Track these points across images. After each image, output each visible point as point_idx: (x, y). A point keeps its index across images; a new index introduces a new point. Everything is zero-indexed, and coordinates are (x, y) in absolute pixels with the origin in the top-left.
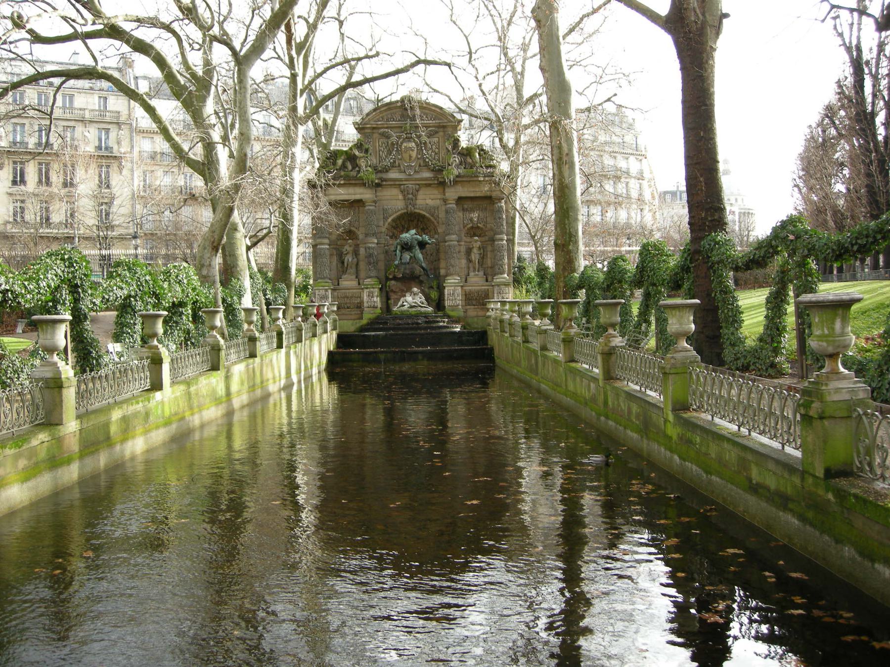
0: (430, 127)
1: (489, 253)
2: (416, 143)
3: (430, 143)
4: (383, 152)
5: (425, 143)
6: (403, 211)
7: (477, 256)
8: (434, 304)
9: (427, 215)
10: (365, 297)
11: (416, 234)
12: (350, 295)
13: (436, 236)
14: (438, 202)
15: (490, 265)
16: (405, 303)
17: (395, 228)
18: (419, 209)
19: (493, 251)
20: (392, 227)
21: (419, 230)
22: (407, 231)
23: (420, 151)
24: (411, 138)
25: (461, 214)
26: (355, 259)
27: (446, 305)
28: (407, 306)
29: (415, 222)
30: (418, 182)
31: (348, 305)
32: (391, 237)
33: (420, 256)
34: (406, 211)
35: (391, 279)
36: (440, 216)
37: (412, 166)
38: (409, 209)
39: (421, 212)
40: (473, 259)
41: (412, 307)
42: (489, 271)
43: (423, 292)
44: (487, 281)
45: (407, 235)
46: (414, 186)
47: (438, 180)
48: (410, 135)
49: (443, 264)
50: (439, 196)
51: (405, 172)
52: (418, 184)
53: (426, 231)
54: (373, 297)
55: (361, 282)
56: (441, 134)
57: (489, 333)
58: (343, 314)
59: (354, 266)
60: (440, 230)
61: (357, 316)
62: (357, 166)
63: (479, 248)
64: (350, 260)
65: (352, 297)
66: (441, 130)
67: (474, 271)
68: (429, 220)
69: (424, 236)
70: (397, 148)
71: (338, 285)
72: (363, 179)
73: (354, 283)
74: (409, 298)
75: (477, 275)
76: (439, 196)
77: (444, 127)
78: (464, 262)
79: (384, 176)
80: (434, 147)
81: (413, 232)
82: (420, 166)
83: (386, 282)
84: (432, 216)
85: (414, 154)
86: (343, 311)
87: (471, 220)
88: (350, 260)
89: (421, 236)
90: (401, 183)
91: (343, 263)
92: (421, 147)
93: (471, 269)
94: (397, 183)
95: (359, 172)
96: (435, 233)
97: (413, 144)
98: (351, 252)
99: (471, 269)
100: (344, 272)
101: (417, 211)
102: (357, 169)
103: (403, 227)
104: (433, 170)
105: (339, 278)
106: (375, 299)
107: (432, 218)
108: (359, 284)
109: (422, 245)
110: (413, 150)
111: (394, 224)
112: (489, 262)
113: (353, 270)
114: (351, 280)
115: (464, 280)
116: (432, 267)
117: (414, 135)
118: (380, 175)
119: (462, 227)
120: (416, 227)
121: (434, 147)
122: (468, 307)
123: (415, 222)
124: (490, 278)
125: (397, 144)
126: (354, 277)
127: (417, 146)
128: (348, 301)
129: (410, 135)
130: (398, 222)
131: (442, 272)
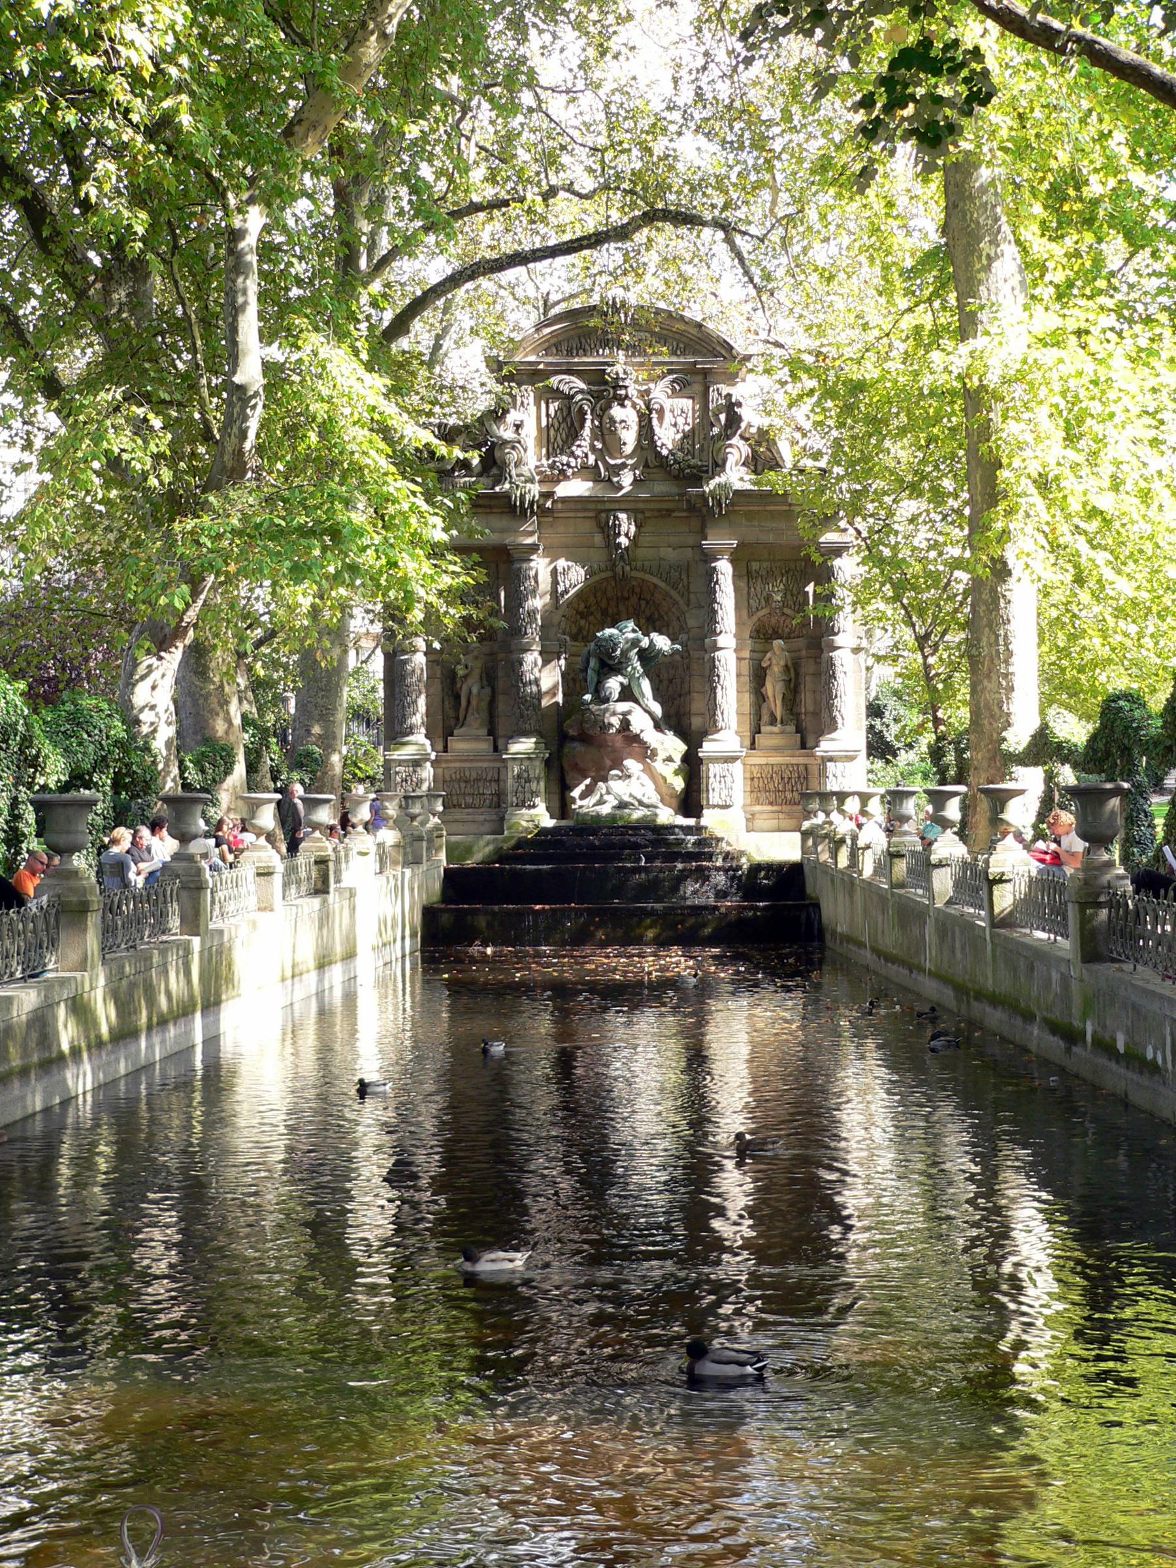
1: (808, 678)
3: (672, 411)
4: (557, 431)
5: (661, 412)
6: (603, 575)
7: (780, 687)
8: (675, 802)
9: (663, 585)
10: (510, 781)
12: (474, 775)
13: (683, 637)
14: (689, 553)
15: (810, 708)
17: (582, 615)
18: (643, 570)
19: (817, 674)
20: (578, 612)
21: (643, 621)
23: (646, 431)
24: (627, 396)
25: (743, 584)
26: (488, 690)
27: (704, 803)
28: (612, 802)
29: (634, 600)
30: (641, 506)
31: (469, 800)
32: (574, 638)
33: (646, 685)
34: (609, 574)
35: (573, 739)
36: (692, 588)
38: (619, 569)
39: (647, 577)
40: (770, 694)
41: (622, 805)
42: (808, 722)
43: (649, 771)
44: (803, 746)
47: (689, 502)
48: (623, 392)
49: (697, 704)
50: (691, 540)
51: (610, 480)
52: (642, 512)
53: (658, 624)
54: (528, 780)
55: (501, 742)
56: (698, 388)
57: (806, 870)
58: (457, 821)
59: (484, 705)
60: (692, 623)
61: (487, 827)
62: (495, 462)
64: (475, 690)
65: (477, 780)
66: (700, 378)
67: (773, 721)
68: (667, 595)
69: (653, 635)
71: (445, 750)
72: (510, 498)
73: (485, 746)
74: (618, 786)
76: (691, 540)
77: (705, 373)
78: (747, 698)
80: (681, 421)
81: (631, 625)
82: (646, 466)
83: (561, 746)
84: (675, 587)
86: (458, 814)
87: (768, 599)
88: (475, 690)
90: (600, 507)
91: (457, 697)
92: (650, 419)
93: (765, 718)
94: (591, 506)
95: (499, 480)
96: (682, 629)
98: (476, 674)
99: (765, 718)
100: (460, 721)
101: (634, 574)
102: (494, 471)
103: (605, 613)
104: (676, 478)
105: (448, 733)
106: (534, 786)
107: (673, 593)
108: (496, 749)
109: (647, 656)
111: (582, 606)
112: (807, 701)
113: (485, 715)
114: (477, 738)
115: (748, 742)
116: (672, 712)
117: (632, 391)
119: (745, 613)
120: (635, 615)
121: (681, 421)
122: (758, 808)
123: (634, 600)
124: (810, 743)
126: (484, 731)
127: (641, 416)
128: (468, 790)
129: (623, 392)
130: (592, 600)
131: (696, 722)
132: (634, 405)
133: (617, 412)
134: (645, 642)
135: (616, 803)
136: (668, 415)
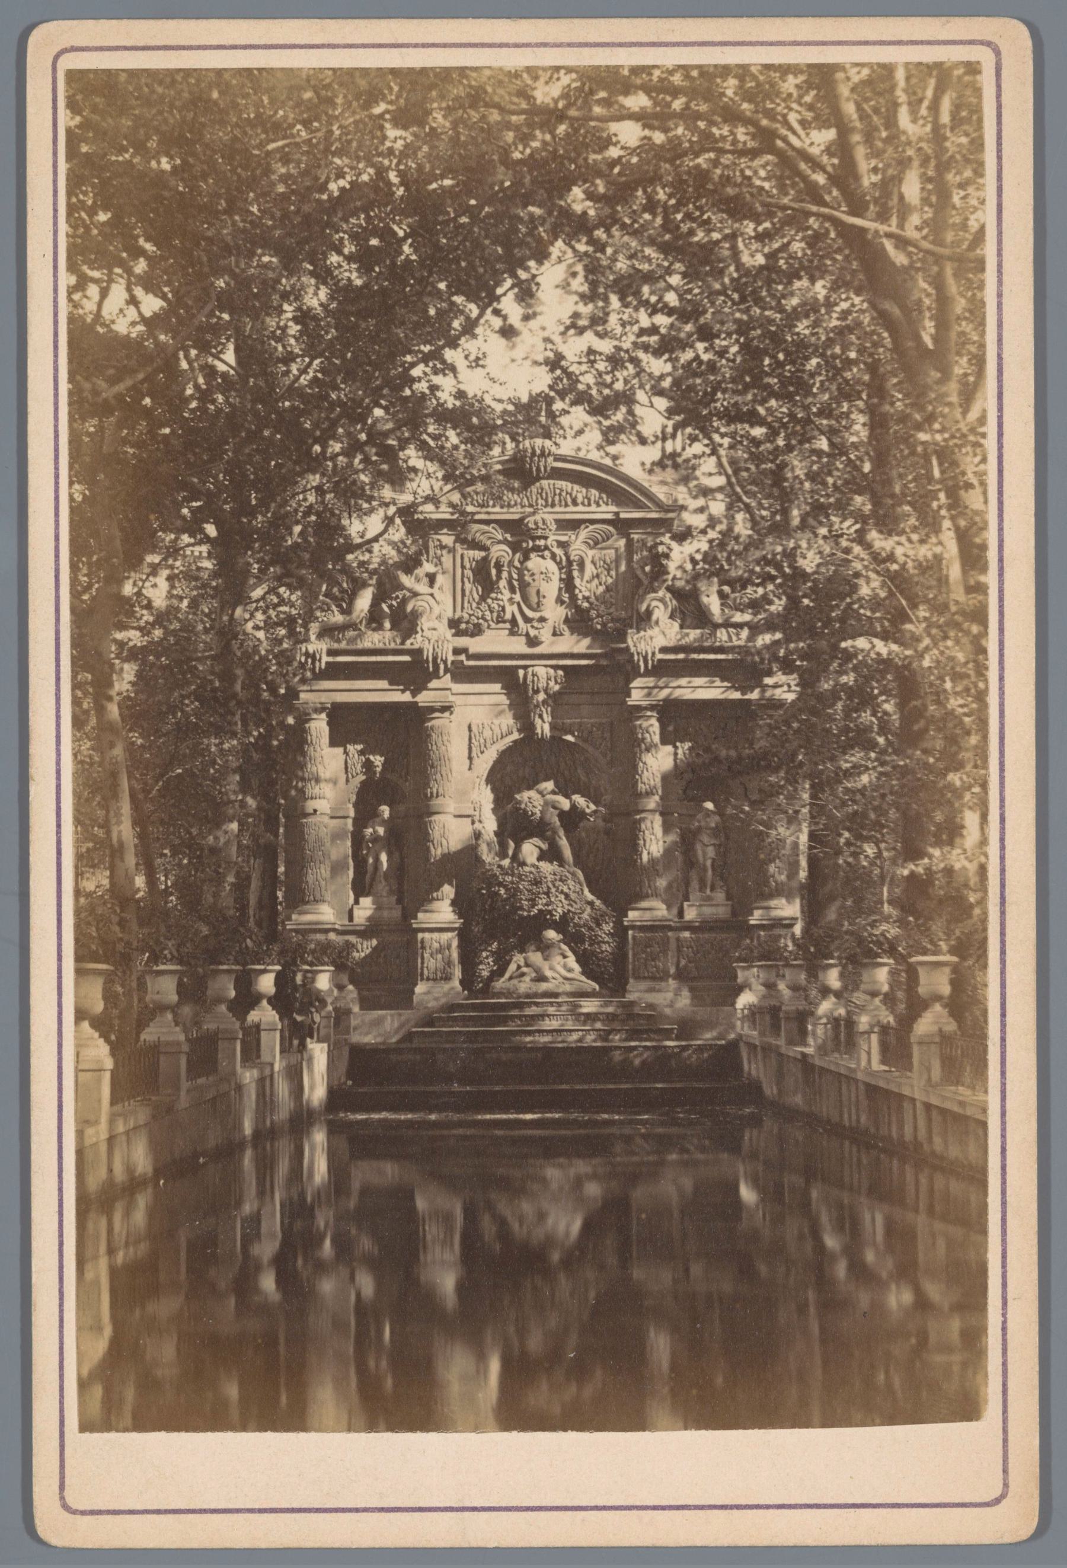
0: (593, 522)
2: (559, 564)
3: (593, 562)
5: (582, 565)
7: (711, 852)
11: (553, 792)
16: (525, 970)
22: (529, 788)
24: (546, 548)
37: (542, 620)
45: (532, 793)
46: (551, 671)
48: (542, 543)
52: (563, 668)
63: (715, 832)
70: (510, 573)
75: (709, 898)
79: (475, 645)
81: (549, 785)
85: (551, 588)
89: (567, 796)
93: (695, 884)
97: (552, 567)
99: (695, 884)
110: (548, 579)
115: (675, 911)
118: (463, 642)
125: (511, 563)
127: (560, 569)
129: (542, 543)
132: (553, 556)
133: (535, 563)
134: (565, 804)
135: (534, 975)
136: (589, 569)
